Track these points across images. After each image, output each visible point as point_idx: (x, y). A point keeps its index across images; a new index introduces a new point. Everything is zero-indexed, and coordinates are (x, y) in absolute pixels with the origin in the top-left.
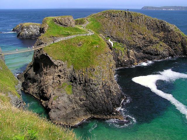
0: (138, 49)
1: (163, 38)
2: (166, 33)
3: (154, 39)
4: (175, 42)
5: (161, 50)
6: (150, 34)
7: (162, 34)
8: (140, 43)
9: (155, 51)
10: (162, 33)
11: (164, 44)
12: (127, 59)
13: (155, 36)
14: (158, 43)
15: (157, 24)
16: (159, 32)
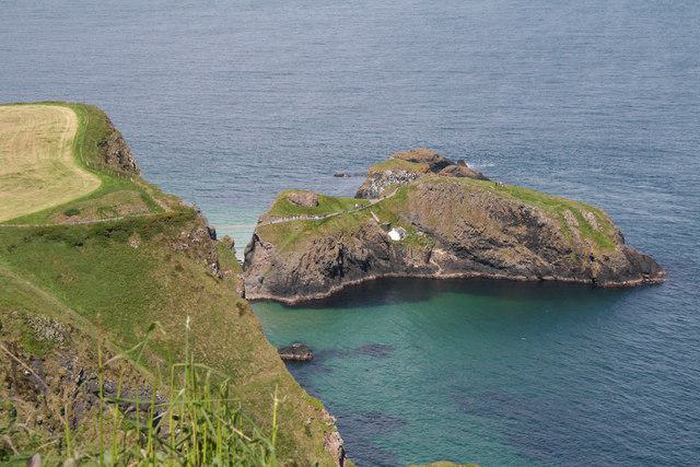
0: (461, 251)
1: (526, 238)
2: (532, 229)
3: (503, 238)
4: (554, 248)
5: (509, 261)
6: (493, 230)
7: (522, 230)
8: (467, 243)
9: (499, 261)
10: (524, 227)
11: (527, 251)
12: (422, 263)
13: (504, 231)
14: (512, 246)
15: (510, 210)
16: (516, 225)
